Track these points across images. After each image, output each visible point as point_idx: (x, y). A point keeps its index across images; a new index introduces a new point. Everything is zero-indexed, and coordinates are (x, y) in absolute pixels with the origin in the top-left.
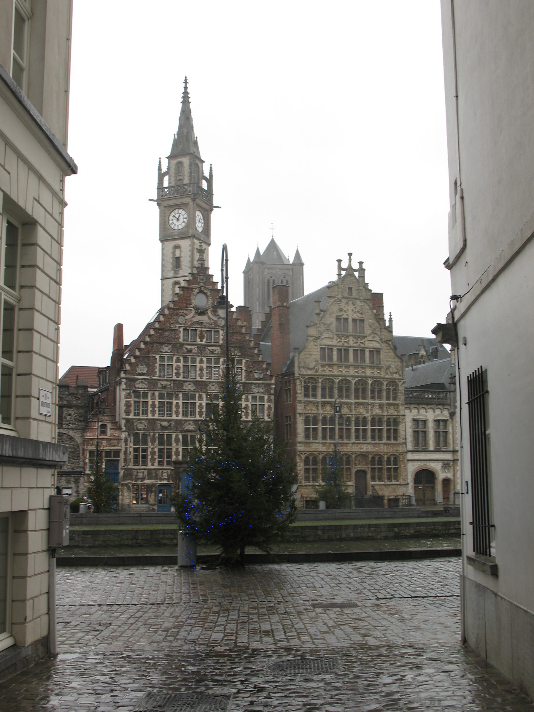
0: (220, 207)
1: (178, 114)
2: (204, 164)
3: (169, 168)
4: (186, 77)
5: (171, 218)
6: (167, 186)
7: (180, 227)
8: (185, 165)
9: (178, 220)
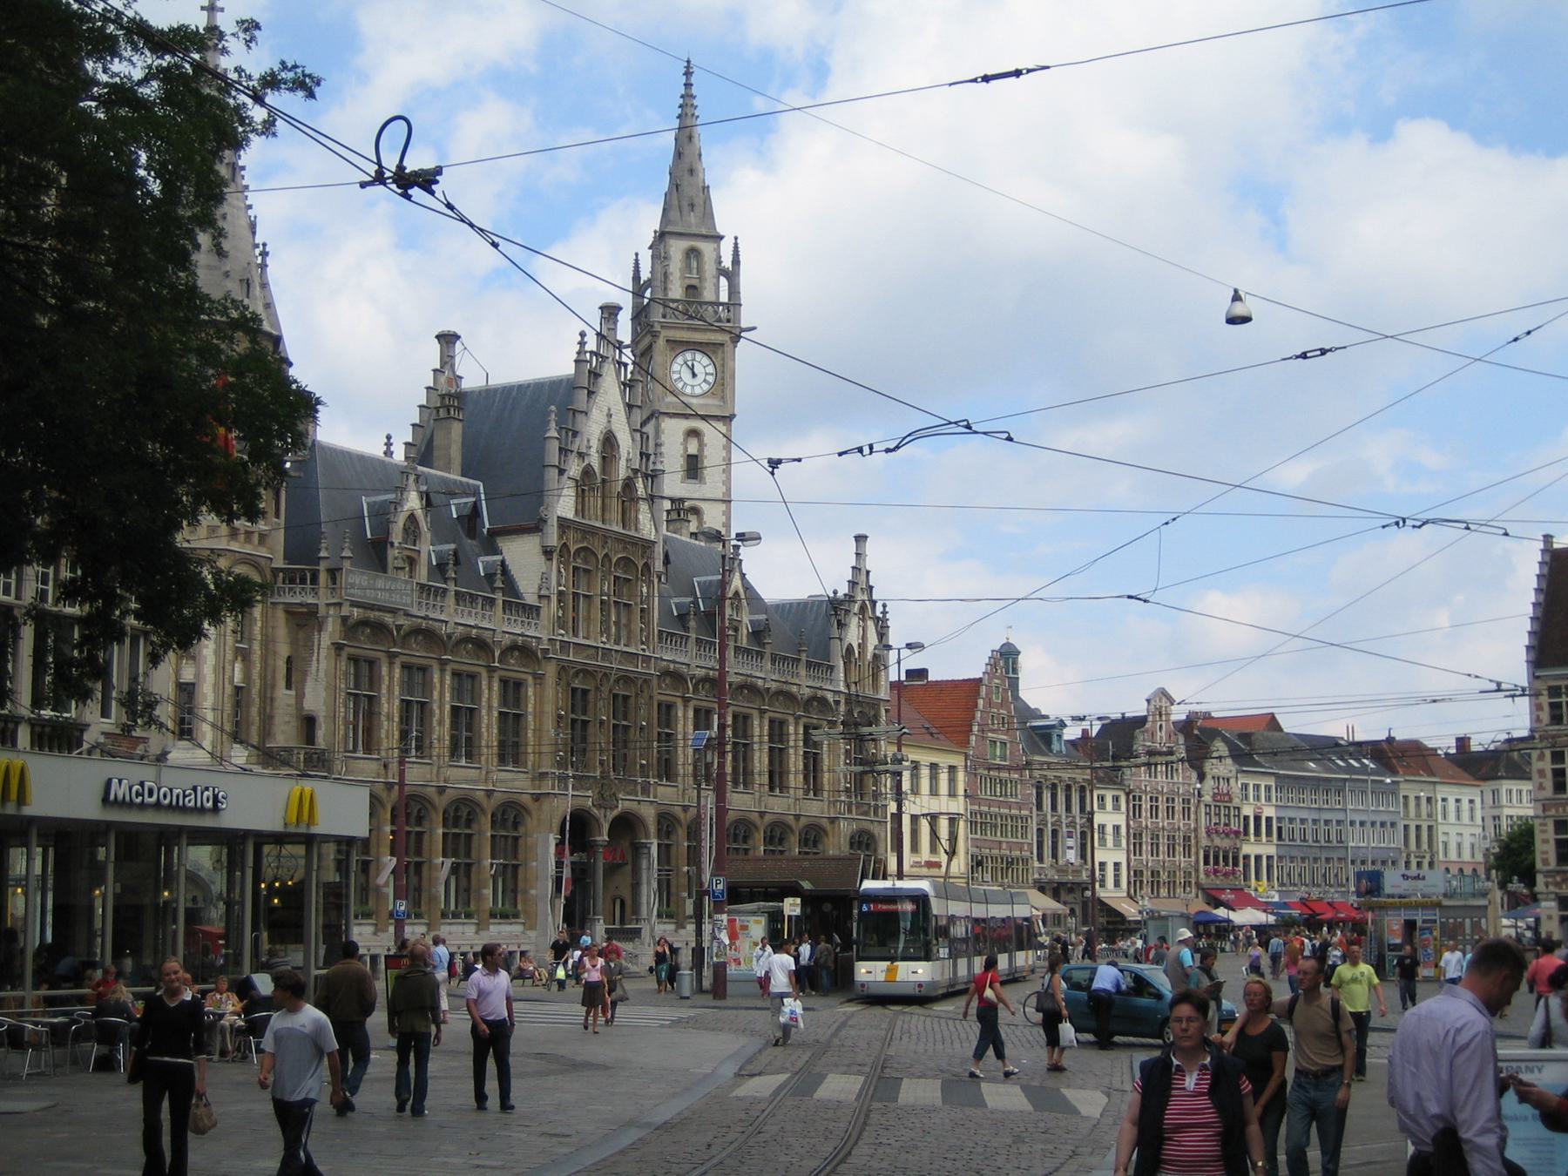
5: (676, 367)
7: (698, 391)
9: (694, 375)
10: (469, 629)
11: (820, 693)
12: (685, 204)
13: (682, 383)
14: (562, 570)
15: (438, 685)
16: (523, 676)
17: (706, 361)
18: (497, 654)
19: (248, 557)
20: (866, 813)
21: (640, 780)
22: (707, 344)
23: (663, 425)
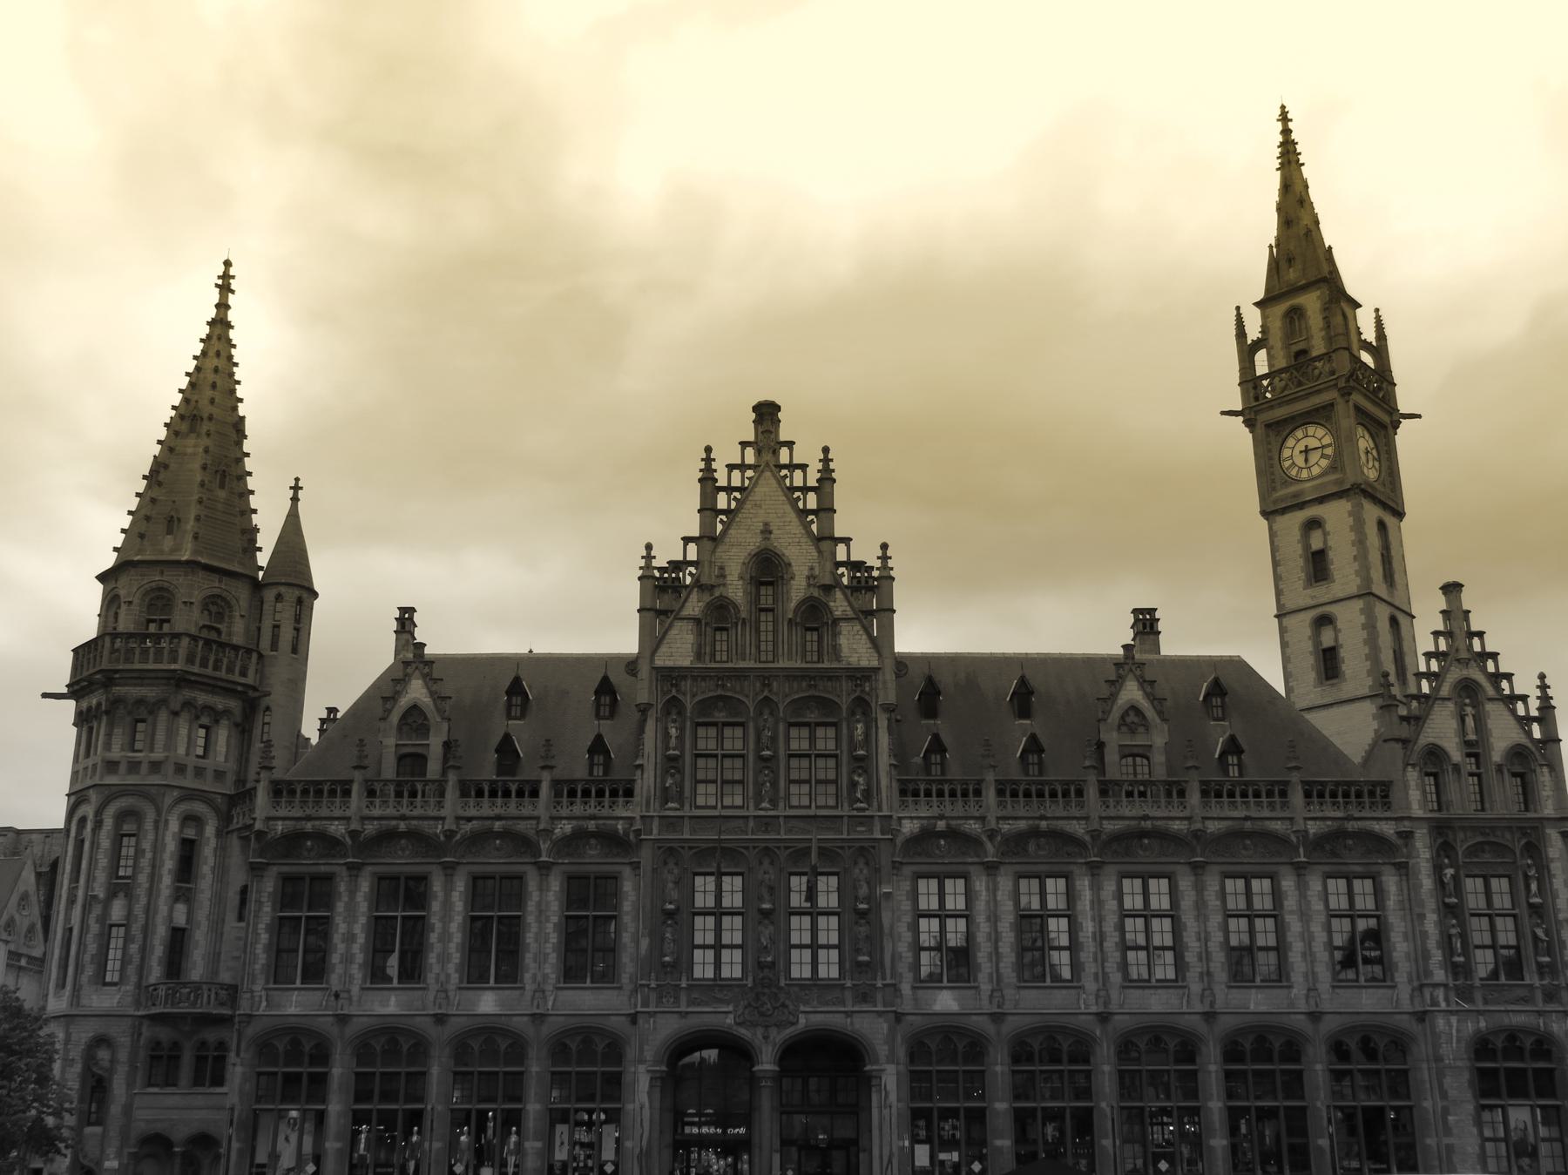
0: (1419, 416)
1: (1274, 196)
2: (1358, 311)
3: (1265, 329)
4: (1283, 107)
5: (1286, 453)
6: (1266, 370)
7: (1316, 471)
8: (1309, 313)
10: (488, 823)
11: (1351, 826)
12: (1283, 265)
13: (1297, 468)
14: (673, 732)
15: (440, 895)
16: (617, 868)
17: (1320, 432)
18: (544, 846)
19: (131, 788)
20: (1525, 1000)
21: (849, 984)
22: (1317, 410)
23: (1275, 527)
